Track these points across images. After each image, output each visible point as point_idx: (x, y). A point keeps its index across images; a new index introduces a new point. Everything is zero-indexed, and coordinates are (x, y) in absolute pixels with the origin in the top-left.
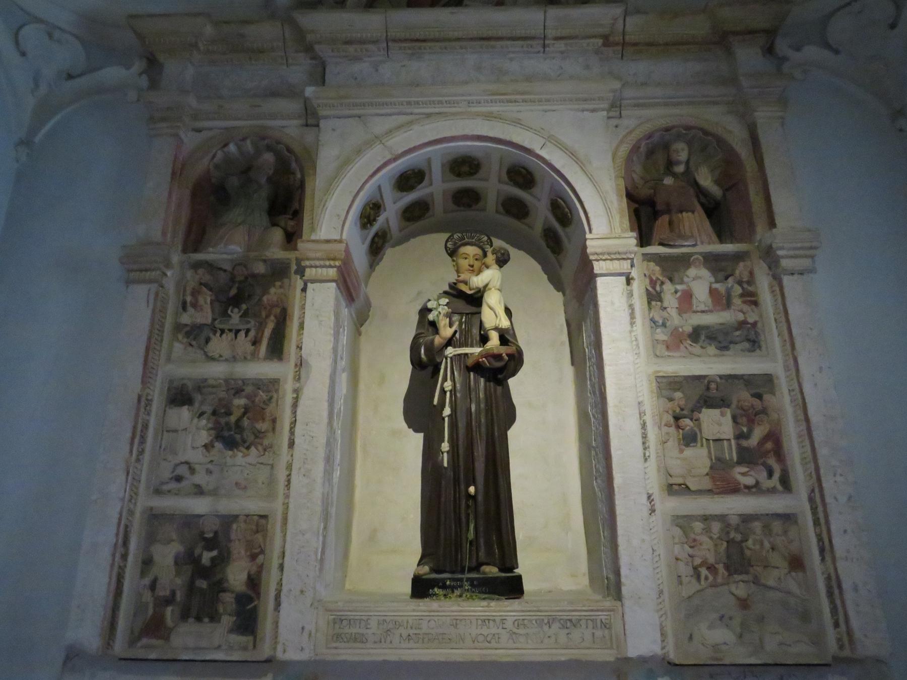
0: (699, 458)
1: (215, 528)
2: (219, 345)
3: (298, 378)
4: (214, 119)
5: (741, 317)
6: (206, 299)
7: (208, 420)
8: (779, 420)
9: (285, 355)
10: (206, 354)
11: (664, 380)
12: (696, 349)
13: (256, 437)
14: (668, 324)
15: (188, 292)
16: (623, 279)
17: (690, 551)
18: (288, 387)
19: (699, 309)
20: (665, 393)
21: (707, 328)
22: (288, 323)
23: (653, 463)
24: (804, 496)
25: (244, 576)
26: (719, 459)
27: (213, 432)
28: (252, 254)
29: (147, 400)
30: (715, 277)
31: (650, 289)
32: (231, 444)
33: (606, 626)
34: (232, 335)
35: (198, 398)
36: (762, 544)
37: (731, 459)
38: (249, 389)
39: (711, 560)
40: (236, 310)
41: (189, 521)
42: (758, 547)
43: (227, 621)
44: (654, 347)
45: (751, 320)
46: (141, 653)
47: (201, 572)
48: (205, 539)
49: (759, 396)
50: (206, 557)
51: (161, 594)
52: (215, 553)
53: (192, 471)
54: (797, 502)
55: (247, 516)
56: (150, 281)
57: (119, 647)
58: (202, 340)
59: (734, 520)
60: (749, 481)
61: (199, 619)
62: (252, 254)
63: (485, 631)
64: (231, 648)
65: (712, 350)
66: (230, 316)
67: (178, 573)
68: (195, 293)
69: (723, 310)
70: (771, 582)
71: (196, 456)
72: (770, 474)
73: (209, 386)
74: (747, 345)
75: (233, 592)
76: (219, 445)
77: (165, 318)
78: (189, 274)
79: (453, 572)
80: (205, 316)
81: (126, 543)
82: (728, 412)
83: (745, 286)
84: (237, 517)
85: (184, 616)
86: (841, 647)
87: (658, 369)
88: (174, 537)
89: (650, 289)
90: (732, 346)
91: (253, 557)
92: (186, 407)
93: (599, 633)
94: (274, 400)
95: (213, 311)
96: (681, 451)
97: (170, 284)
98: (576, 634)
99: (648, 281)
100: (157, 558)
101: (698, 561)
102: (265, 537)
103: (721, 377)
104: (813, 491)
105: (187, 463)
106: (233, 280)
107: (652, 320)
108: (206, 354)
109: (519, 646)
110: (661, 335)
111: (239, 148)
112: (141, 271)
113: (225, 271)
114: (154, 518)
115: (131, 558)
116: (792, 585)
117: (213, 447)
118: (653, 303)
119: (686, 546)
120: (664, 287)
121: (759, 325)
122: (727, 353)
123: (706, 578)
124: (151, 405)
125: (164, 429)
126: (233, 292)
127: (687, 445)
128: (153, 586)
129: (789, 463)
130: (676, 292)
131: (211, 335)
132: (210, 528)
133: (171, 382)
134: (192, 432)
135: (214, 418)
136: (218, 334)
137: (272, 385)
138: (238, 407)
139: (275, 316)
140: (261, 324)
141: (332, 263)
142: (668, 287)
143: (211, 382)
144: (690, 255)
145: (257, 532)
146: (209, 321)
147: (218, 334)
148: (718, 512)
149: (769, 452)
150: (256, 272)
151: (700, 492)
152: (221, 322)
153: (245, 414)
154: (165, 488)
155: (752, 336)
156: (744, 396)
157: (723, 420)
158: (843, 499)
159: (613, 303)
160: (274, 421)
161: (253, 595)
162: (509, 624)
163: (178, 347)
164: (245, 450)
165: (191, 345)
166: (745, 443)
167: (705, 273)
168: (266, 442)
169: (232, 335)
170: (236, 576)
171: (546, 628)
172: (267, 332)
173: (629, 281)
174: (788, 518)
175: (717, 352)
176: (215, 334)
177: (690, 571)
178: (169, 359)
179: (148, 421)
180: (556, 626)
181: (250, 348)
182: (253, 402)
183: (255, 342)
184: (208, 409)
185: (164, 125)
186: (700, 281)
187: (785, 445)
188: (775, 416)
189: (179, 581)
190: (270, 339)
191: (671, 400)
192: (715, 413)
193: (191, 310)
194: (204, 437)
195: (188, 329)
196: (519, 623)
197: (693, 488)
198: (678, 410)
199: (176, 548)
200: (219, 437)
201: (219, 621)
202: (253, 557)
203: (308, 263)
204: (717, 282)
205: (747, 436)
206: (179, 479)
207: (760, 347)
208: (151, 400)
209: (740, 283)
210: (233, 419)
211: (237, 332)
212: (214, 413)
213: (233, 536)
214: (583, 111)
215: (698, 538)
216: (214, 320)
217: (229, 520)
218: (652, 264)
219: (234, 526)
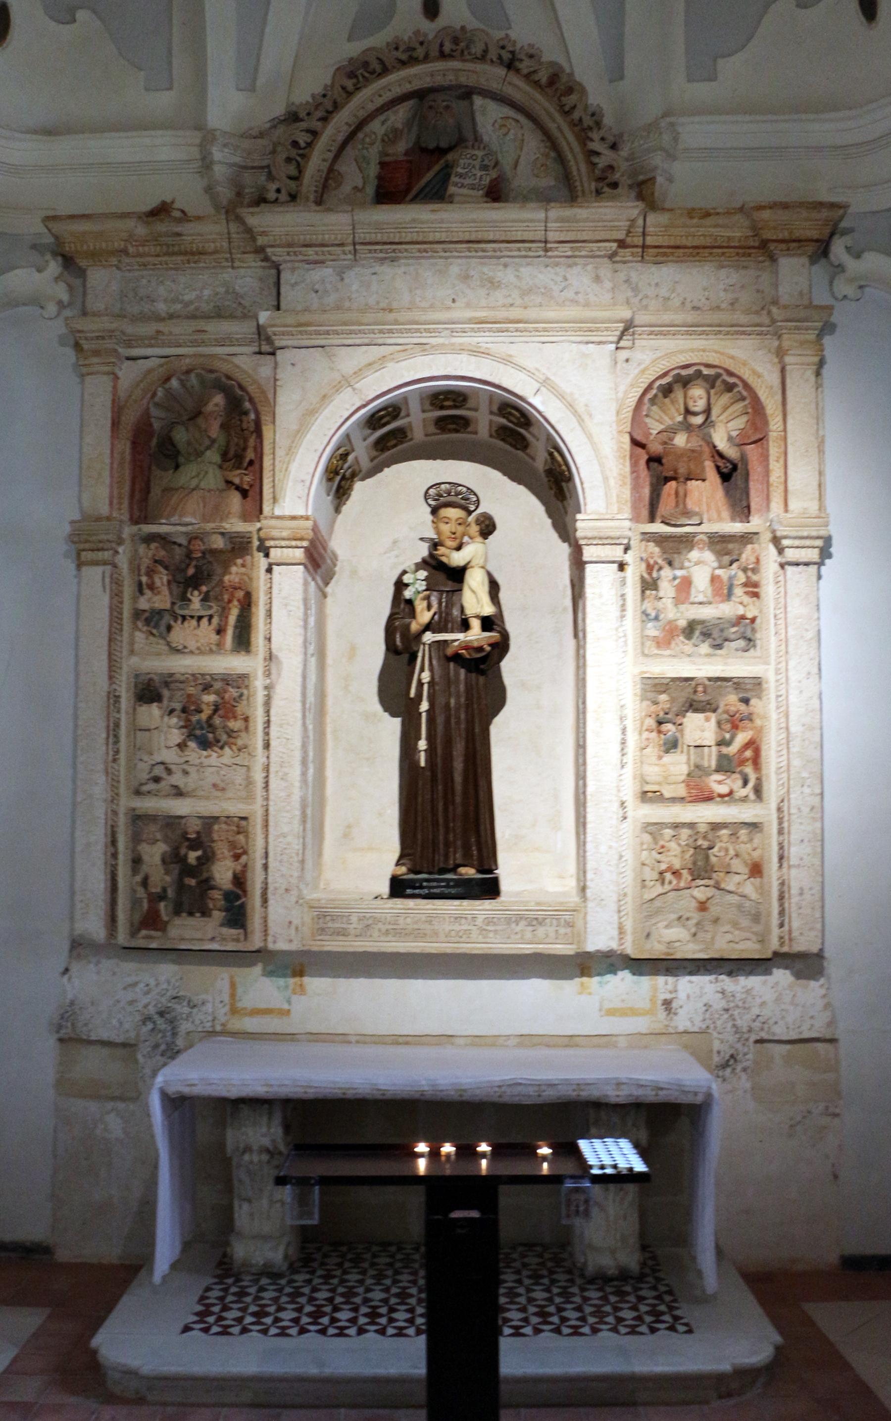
0: (678, 765)
1: (197, 828)
2: (181, 634)
3: (268, 674)
4: (152, 346)
5: (741, 611)
6: (162, 578)
8: (762, 727)
9: (253, 648)
10: (168, 644)
11: (649, 681)
12: (688, 647)
13: (230, 736)
14: (662, 616)
15: (143, 571)
16: (616, 566)
17: (659, 857)
18: (259, 683)
19: (696, 600)
20: (651, 695)
21: (702, 622)
22: (254, 609)
23: (629, 771)
24: (773, 806)
25: (230, 875)
26: (697, 767)
27: (184, 730)
28: (209, 526)
30: (719, 561)
31: (646, 576)
32: (205, 744)
33: (570, 925)
34: (194, 622)
35: (166, 693)
36: (727, 850)
37: (709, 767)
38: (218, 685)
39: (677, 866)
40: (196, 593)
41: (172, 822)
42: (722, 854)
43: (218, 915)
44: (643, 644)
45: (750, 615)
46: (141, 943)
47: (187, 870)
48: (188, 839)
49: (746, 701)
50: (193, 856)
51: (153, 890)
52: (199, 853)
53: (169, 771)
54: (763, 812)
55: (228, 817)
56: (105, 563)
57: (122, 937)
58: (163, 628)
59: (702, 828)
60: (723, 789)
61: (191, 914)
62: (209, 526)
63: (457, 927)
64: (224, 939)
65: (705, 648)
66: (190, 600)
67: (167, 872)
68: (150, 573)
69: (723, 601)
70: (731, 887)
71: (170, 756)
72: (745, 783)
73: (176, 681)
74: (742, 643)
75: (220, 890)
76: (192, 744)
77: (121, 603)
78: (142, 549)
79: (430, 873)
80: (162, 600)
81: (114, 842)
82: (713, 717)
83: (750, 573)
84: (218, 818)
85: (177, 911)
86: (782, 944)
87: (645, 669)
88: (159, 836)
89: (646, 576)
90: (726, 643)
91: (237, 857)
92: (155, 704)
93: (562, 931)
94: (244, 698)
95: (171, 593)
96: (660, 758)
97: (123, 560)
98: (541, 931)
99: (644, 566)
100: (146, 858)
101: (663, 867)
102: (247, 837)
103: (710, 679)
104: (782, 801)
105: (162, 763)
106: (189, 555)
107: (645, 613)
108: (168, 644)
109: (488, 940)
110: (652, 630)
111: (182, 383)
112: (92, 550)
113: (180, 545)
114: (138, 819)
115: (121, 857)
116: (749, 889)
118: (648, 592)
119: (654, 853)
120: (662, 573)
121: (758, 621)
122: (719, 652)
123: (670, 883)
126: (191, 571)
127: (667, 751)
128: (145, 883)
129: (764, 772)
130: (675, 578)
131: (172, 623)
132: (193, 827)
133: (137, 676)
134: (165, 731)
135: (184, 715)
136: (179, 622)
137: (241, 681)
138: (207, 704)
139: (239, 600)
140: (224, 608)
141: (299, 543)
142: (667, 573)
143: (178, 676)
144: (695, 534)
145: (239, 833)
146: (168, 606)
147: (179, 622)
148: (688, 821)
149: (747, 760)
150: (215, 546)
151: (673, 800)
152: (181, 608)
153: (215, 711)
154: (145, 788)
155: (749, 634)
156: (731, 700)
157: (707, 724)
158: (805, 810)
159: (601, 596)
160: (246, 719)
161: (240, 892)
162: (479, 921)
163: (139, 636)
165: (153, 635)
166: (725, 750)
167: (709, 556)
168: (240, 742)
169: (194, 622)
170: (222, 873)
171: (513, 925)
172: (232, 619)
173: (622, 566)
174: (754, 826)
175: (710, 650)
176: (175, 621)
177: (655, 876)
178: (132, 652)
180: (523, 923)
181: (215, 638)
183: (220, 631)
184: (178, 706)
185: (95, 360)
186: (701, 565)
187: (763, 753)
188: (758, 722)
189: (168, 878)
190: (236, 627)
191: (656, 703)
192: (701, 716)
193: (148, 593)
194: (176, 736)
195: (147, 615)
196: (489, 921)
197: (667, 795)
198: (661, 714)
199: (161, 848)
200: (191, 736)
201: (210, 916)
202: (237, 857)
203: (272, 543)
204: (720, 567)
206: (157, 780)
207: (754, 646)
208: (119, 697)
209: (745, 570)
210: (204, 716)
211: (200, 618)
212: (184, 710)
213: (215, 836)
214: (587, 343)
215: (667, 844)
216: (173, 604)
217: (210, 821)
218: (652, 544)
219: (216, 827)
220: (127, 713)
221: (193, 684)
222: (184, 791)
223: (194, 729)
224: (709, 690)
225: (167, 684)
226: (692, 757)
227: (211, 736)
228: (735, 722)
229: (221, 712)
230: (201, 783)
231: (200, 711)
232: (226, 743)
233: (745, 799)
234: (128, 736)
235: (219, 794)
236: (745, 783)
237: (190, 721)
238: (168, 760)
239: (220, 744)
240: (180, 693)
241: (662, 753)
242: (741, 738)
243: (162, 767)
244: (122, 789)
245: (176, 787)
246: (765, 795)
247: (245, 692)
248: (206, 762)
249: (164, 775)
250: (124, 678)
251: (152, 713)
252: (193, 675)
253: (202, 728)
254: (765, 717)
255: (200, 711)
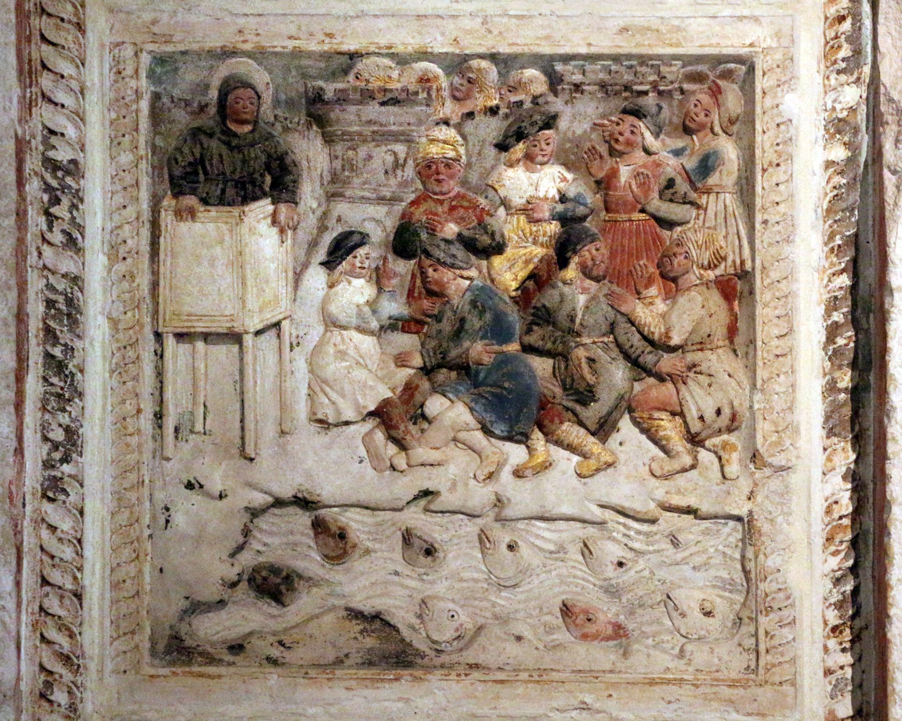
7: (379, 277)
27: (407, 341)
29: (53, 165)
32: (515, 411)
35: (311, 154)
38: (578, 118)
53: (335, 542)
71: (340, 468)
73: (367, 95)
76: (451, 411)
92: (264, 206)
94: (726, 176)
105: (304, 503)
117: (421, 417)
124: (78, 197)
125: (161, 329)
133: (165, 64)
135: (403, 267)
138: (528, 210)
143: (376, 71)
153: (563, 250)
154: (211, 628)
160: (736, 287)
164: (591, 443)
168: (699, 400)
179: (76, 280)
182: (604, 184)
184: (376, 222)
194: (367, 370)
200: (445, 366)
206: (273, 584)
208: (74, 169)
210: (508, 272)
212: (404, 242)
220: (115, 253)
221: (449, 109)
222: (420, 644)
223: (459, 332)
225: (316, 111)
227: (542, 366)
229: (594, 252)
230: (503, 600)
231: (485, 247)
232: (627, 405)
234: (123, 368)
235: (601, 656)
237: (435, 293)
238: (329, 486)
239: (593, 412)
240: (382, 156)
243: (302, 520)
244: (95, 633)
245: (375, 621)
247: (730, 151)
248: (522, 496)
249: (309, 560)
250: (97, 73)
251: (247, 258)
252: (458, 64)
253: (498, 331)
255: (485, 247)
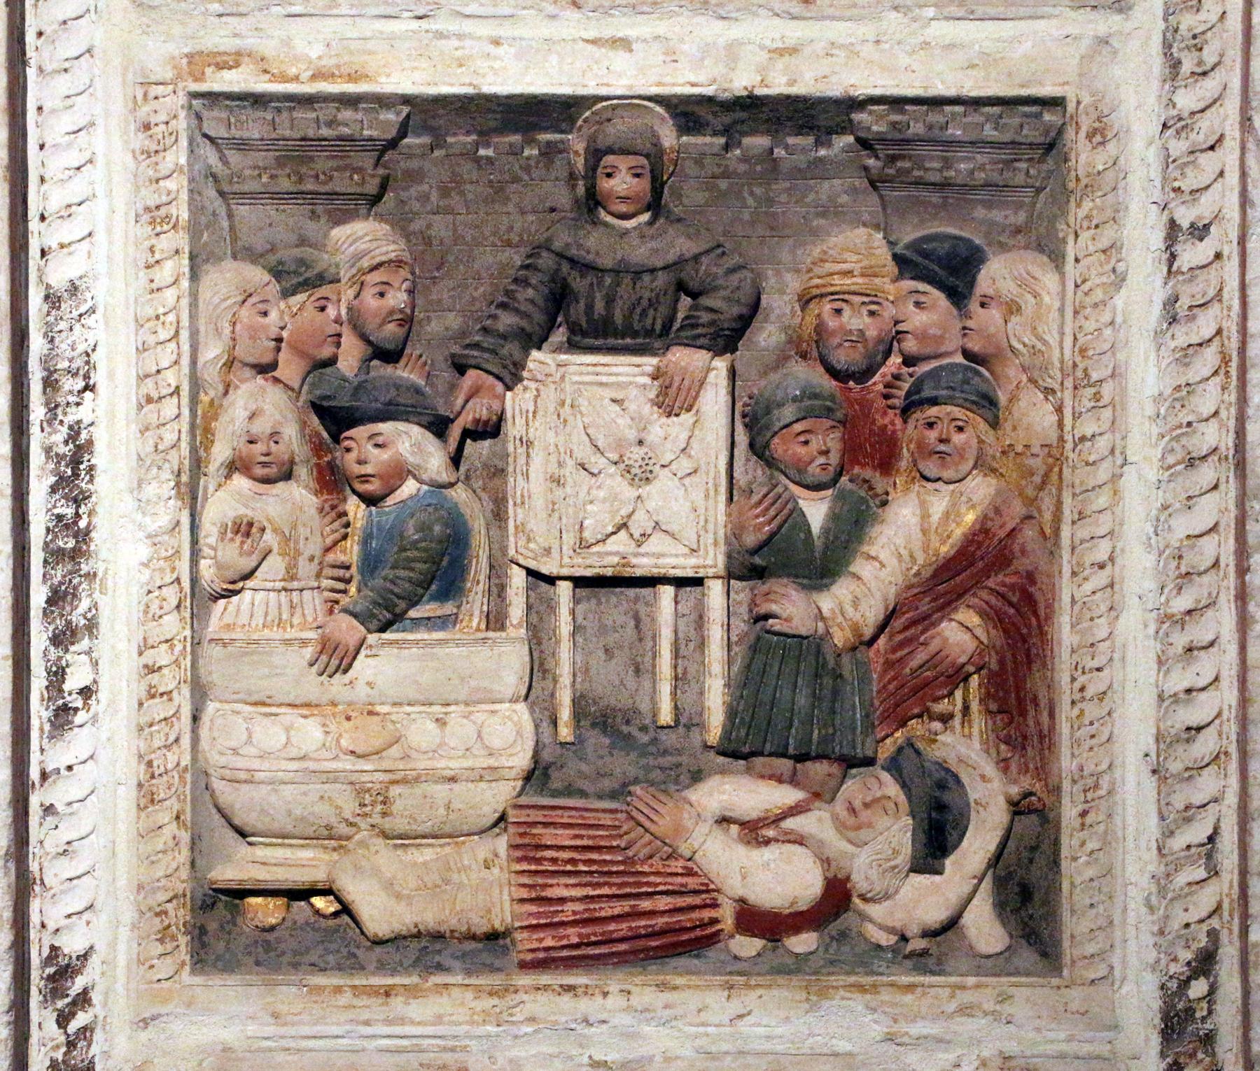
0: (463, 709)
24: (1138, 1002)
26: (598, 717)
37: (687, 721)
49: (952, 270)
60: (781, 878)
72: (936, 839)
96: (336, 658)
103: (689, 112)
127: (387, 616)
149: (958, 677)
151: (427, 950)
156: (845, 258)
157: (668, 433)
166: (794, 608)
188: (1033, 417)
197: (379, 912)
198: (350, 358)
205: (822, 565)
224: (689, 194)
226: (564, 660)
228: (870, 418)
233: (935, 947)
236: (936, 839)
241: (347, 629)
242: (912, 527)
246: (1075, 925)
254: (1085, 379)
